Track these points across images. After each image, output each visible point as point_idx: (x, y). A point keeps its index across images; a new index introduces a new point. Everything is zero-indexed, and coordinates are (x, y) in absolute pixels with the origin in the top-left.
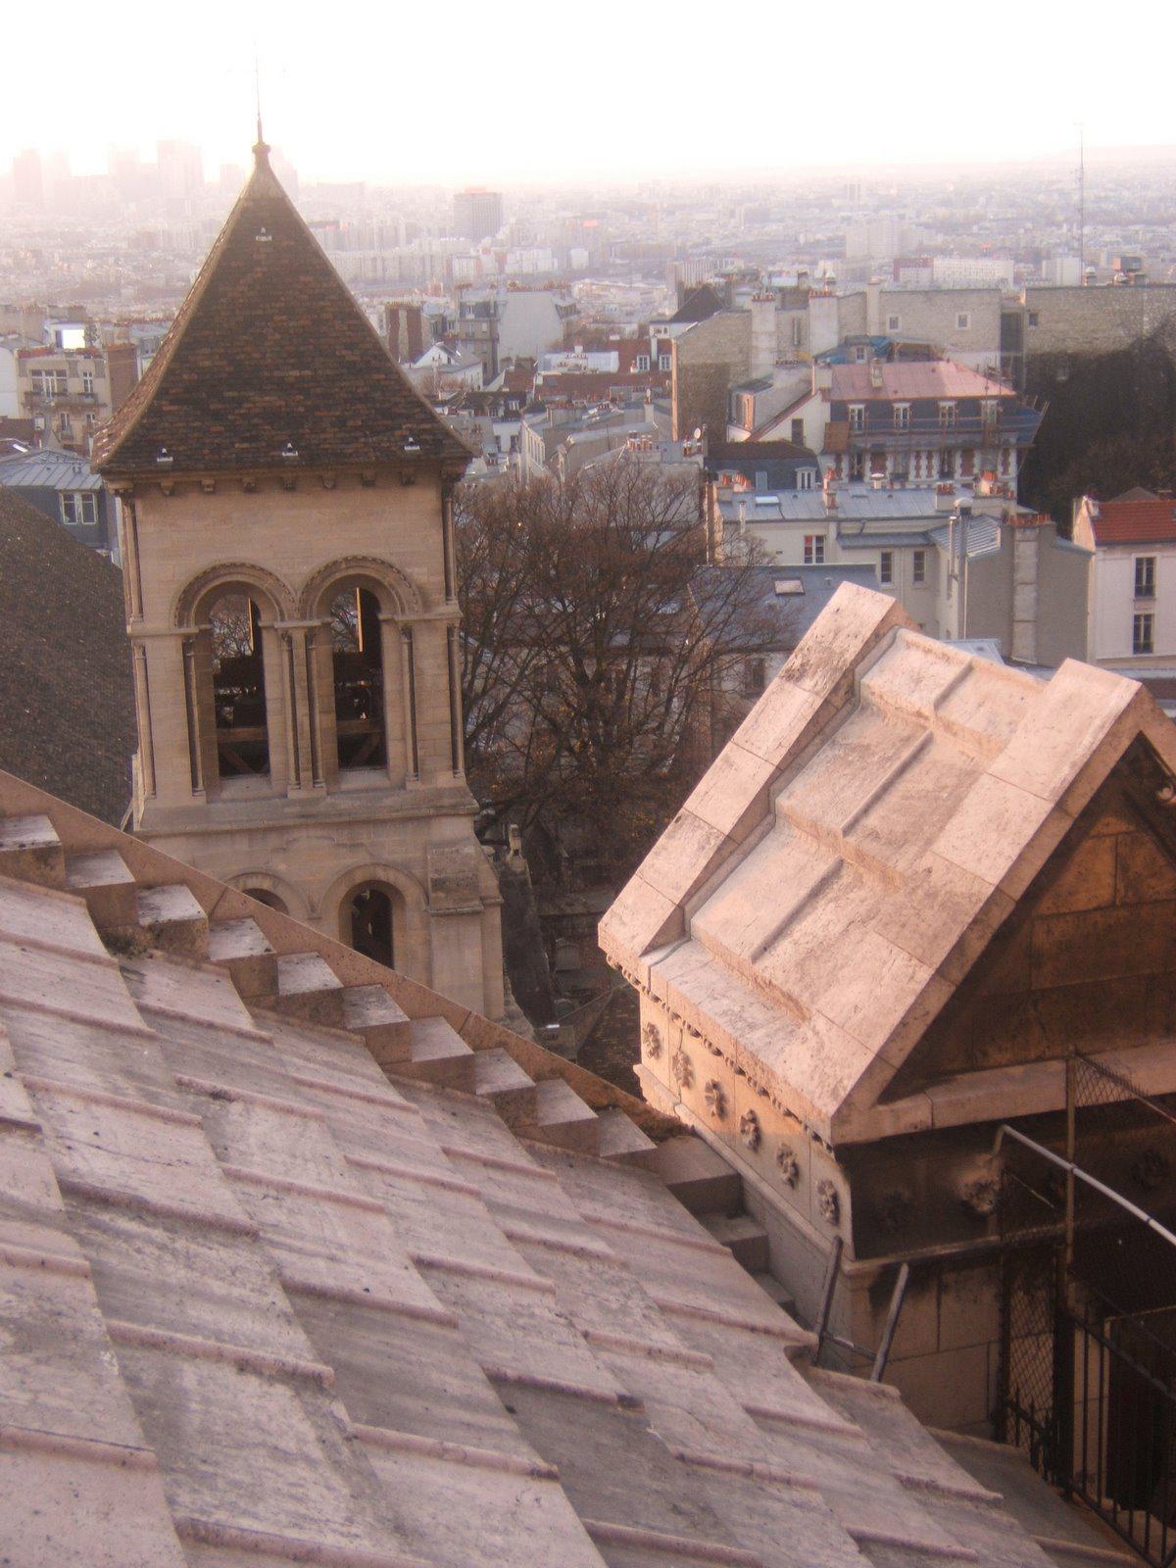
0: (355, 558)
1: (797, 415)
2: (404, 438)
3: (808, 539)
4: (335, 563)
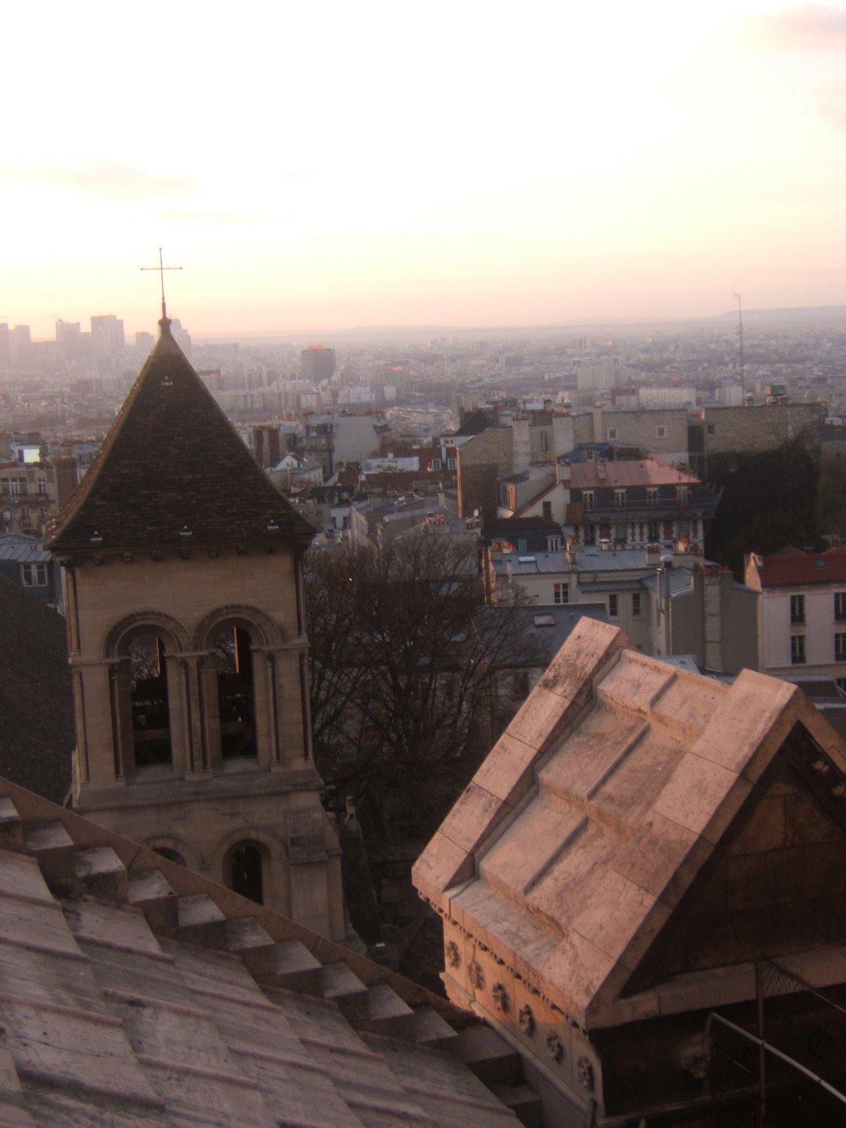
0: (233, 606)
1: (546, 498)
2: (267, 521)
3: (557, 586)
4: (219, 610)
